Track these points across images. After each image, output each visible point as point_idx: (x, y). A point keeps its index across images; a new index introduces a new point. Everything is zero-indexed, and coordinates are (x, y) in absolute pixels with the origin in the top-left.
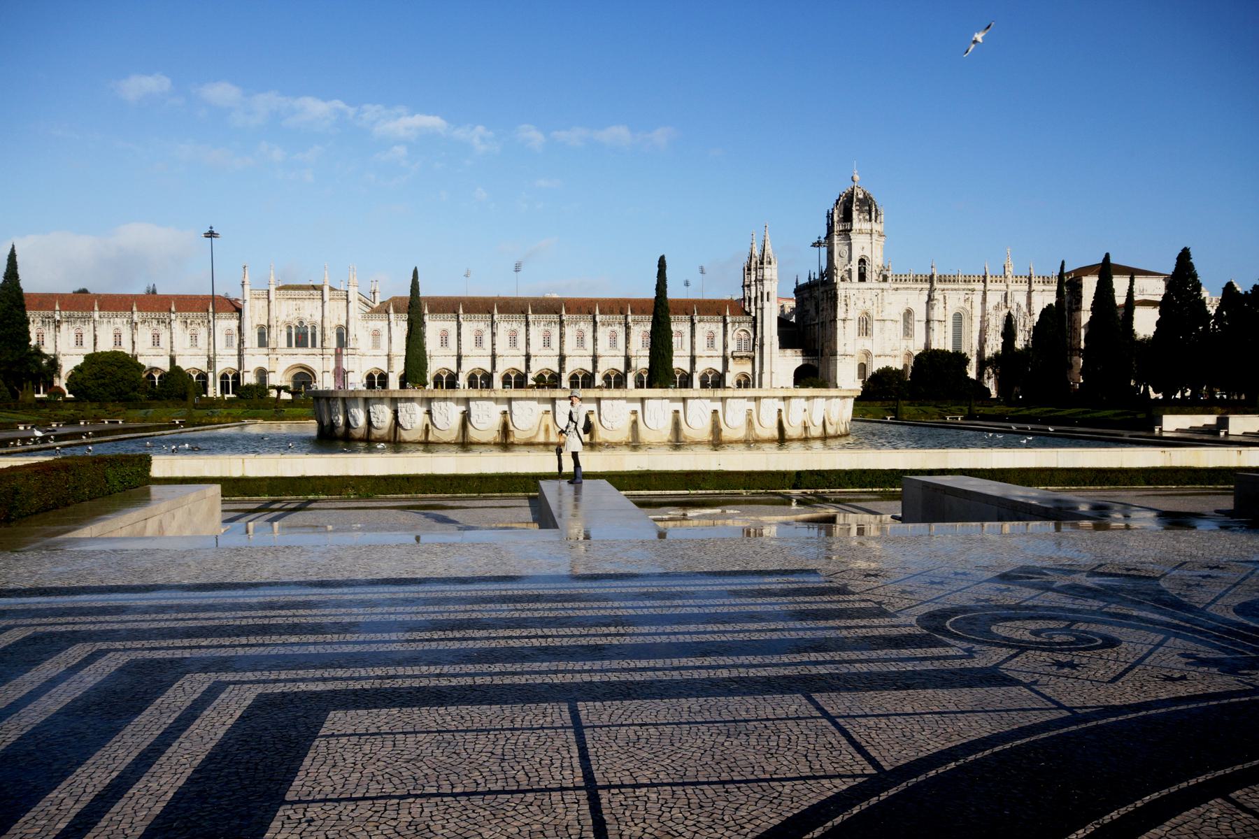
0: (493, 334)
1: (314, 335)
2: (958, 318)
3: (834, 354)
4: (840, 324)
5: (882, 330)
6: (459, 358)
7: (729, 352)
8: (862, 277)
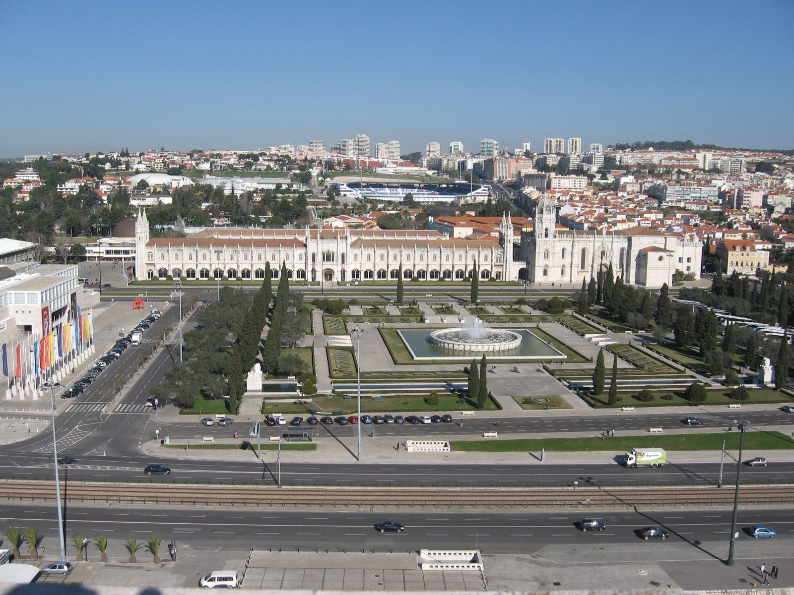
0: (401, 256)
1: (333, 256)
2: (584, 251)
3: (535, 266)
4: (537, 255)
5: (553, 257)
6: (388, 265)
7: (493, 264)
8: (546, 236)
